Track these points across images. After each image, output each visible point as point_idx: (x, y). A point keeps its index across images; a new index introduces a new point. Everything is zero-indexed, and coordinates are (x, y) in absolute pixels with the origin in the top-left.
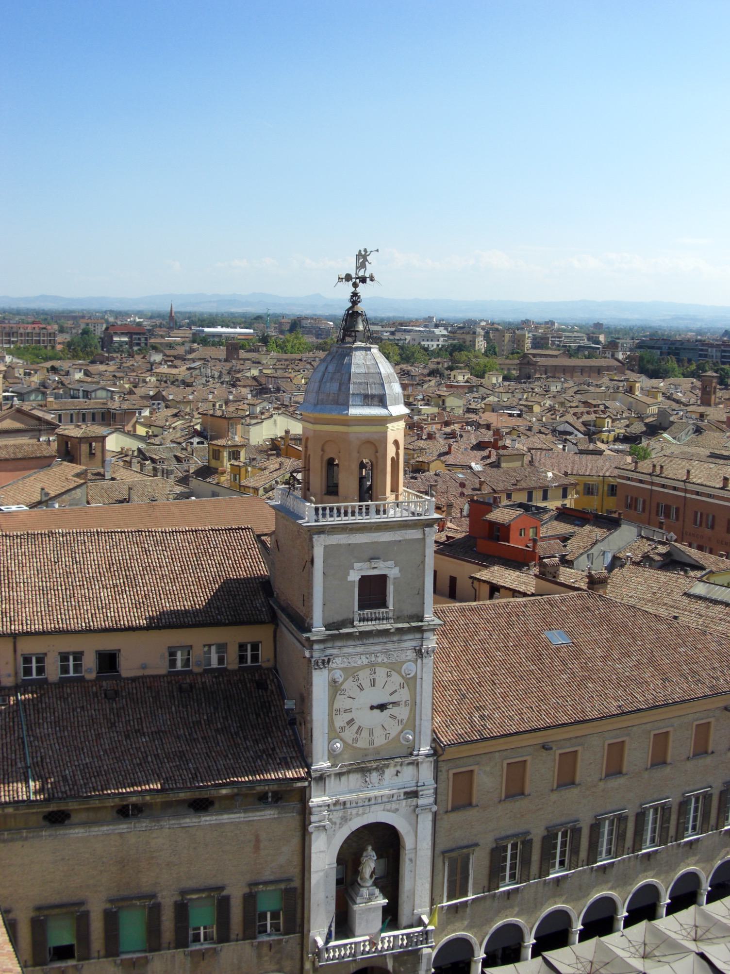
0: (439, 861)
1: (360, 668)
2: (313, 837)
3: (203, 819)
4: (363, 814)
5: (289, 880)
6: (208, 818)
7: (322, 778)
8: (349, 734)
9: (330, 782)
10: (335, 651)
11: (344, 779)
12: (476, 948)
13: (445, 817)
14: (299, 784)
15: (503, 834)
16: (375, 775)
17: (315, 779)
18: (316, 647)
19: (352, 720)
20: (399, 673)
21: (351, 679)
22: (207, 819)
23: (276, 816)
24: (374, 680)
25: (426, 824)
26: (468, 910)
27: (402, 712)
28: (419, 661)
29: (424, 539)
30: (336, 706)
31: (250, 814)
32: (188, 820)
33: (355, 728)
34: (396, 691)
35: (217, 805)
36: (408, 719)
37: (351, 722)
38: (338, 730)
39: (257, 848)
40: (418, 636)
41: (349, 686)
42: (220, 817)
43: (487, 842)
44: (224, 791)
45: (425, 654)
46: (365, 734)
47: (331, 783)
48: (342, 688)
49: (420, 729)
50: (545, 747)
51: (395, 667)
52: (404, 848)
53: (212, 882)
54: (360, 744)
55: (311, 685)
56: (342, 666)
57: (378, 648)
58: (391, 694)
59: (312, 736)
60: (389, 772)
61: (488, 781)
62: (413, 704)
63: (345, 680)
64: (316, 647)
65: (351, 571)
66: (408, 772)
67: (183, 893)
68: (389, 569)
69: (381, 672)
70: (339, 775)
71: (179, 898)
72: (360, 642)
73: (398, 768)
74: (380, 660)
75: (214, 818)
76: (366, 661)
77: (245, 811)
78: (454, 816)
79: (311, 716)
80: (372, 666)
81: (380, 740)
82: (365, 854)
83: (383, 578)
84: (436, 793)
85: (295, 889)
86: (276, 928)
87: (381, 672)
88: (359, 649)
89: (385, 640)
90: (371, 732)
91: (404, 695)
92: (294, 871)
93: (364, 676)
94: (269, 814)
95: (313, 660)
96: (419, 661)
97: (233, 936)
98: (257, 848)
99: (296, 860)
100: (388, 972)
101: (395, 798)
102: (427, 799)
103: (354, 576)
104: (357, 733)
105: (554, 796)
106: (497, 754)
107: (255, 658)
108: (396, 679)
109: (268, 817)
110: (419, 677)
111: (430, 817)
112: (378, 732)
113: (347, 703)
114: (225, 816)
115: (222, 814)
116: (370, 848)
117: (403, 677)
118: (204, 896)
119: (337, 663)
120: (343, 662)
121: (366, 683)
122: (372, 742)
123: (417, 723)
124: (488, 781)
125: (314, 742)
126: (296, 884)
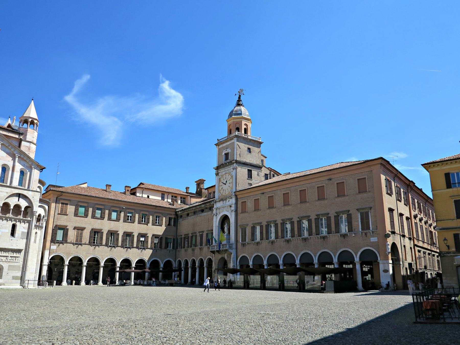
1: (223, 175)
8: (222, 192)
15: (255, 222)
22: (203, 214)
27: (231, 186)
41: (222, 179)
43: (251, 225)
50: (263, 193)
51: (229, 174)
53: (203, 230)
54: (224, 194)
60: (227, 200)
61: (250, 205)
62: (232, 183)
66: (231, 200)
68: (229, 151)
69: (227, 175)
70: (219, 201)
78: (242, 215)
80: (226, 173)
81: (227, 193)
93: (224, 176)
102: (233, 208)
103: (223, 154)
105: (268, 211)
108: (230, 177)
112: (227, 190)
121: (225, 178)
124: (250, 205)
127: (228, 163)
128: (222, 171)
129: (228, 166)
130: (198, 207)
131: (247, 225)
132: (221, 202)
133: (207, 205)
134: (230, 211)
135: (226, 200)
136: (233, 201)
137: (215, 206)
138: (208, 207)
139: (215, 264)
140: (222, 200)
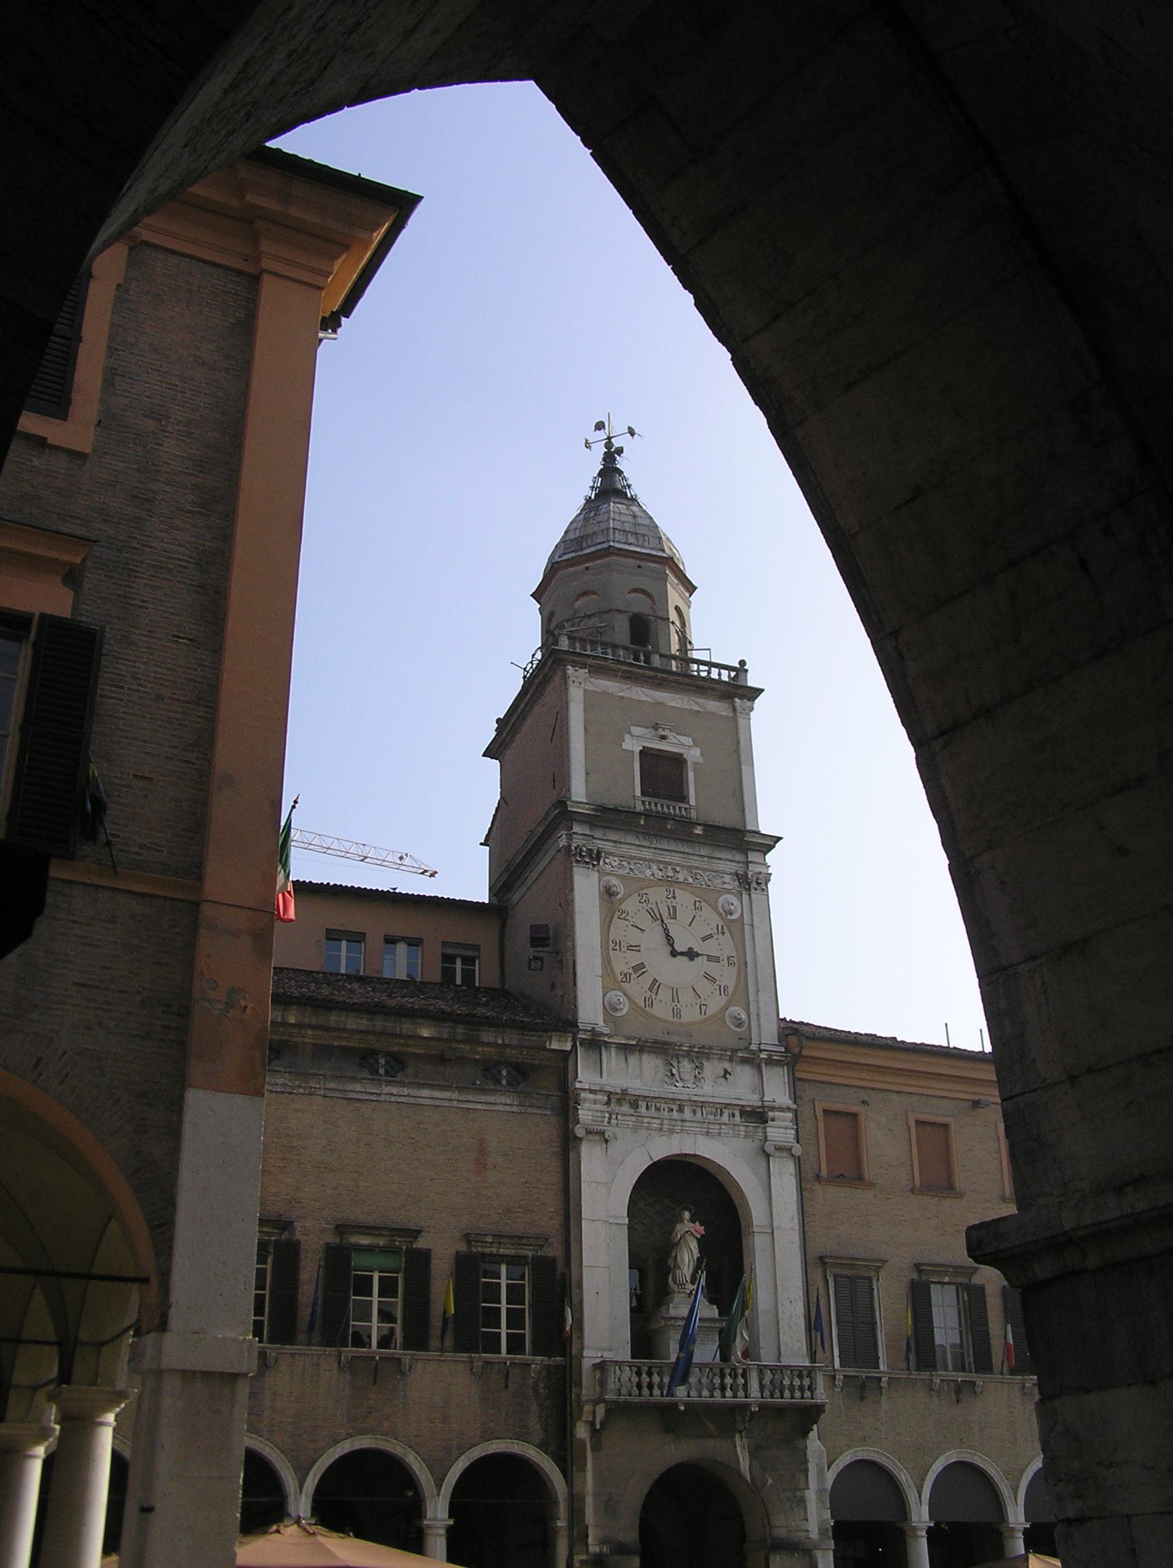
0: (817, 1274)
2: (584, 1149)
3: (386, 1090)
4: (671, 1131)
5: (543, 1240)
6: (394, 1090)
7: (595, 1043)
9: (609, 1061)
10: (607, 846)
11: (633, 1060)
12: (912, 1496)
13: (817, 1187)
14: (555, 1045)
16: (686, 1066)
17: (583, 1042)
18: (577, 828)
19: (642, 965)
20: (716, 909)
21: (635, 897)
23: (515, 1109)
24: (674, 908)
25: (784, 1177)
26: (884, 1399)
28: (745, 897)
29: (735, 718)
30: (613, 935)
31: (470, 1097)
32: (358, 1087)
33: (647, 980)
34: (711, 936)
35: (410, 1071)
36: (736, 988)
37: (640, 968)
38: (620, 978)
39: (481, 1165)
40: (739, 857)
42: (414, 1092)
44: (425, 1033)
45: (754, 885)
46: (664, 994)
47: (611, 1059)
48: (622, 907)
49: (758, 1008)
51: (706, 896)
52: (750, 1224)
55: (572, 890)
56: (620, 872)
57: (677, 859)
58: (704, 939)
59: (575, 974)
60: (712, 1068)
63: (628, 896)
64: (577, 828)
65: (627, 736)
66: (743, 1075)
67: (341, 1229)
70: (625, 1049)
71: (333, 1239)
72: (647, 843)
73: (727, 1065)
74: (681, 877)
75: (406, 1091)
76: (659, 874)
77: (460, 1089)
79: (573, 941)
81: (690, 1015)
82: (678, 1227)
83: (677, 761)
84: (796, 1120)
85: (552, 1261)
86: (516, 1344)
87: (684, 899)
88: (647, 854)
89: (687, 850)
90: (675, 995)
91: (723, 946)
92: (548, 1222)
94: (503, 1102)
95: (574, 845)
96: (745, 897)
97: (435, 1342)
98: (481, 1165)
99: (552, 1203)
100: (741, 1476)
101: (725, 1118)
102: (780, 1131)
103: (633, 745)
104: (650, 989)
106: (894, 1096)
107: (468, 975)
108: (709, 920)
109: (502, 1108)
110: (746, 919)
111: (790, 1167)
112: (686, 997)
113: (633, 937)
114: (425, 1092)
115: (420, 1086)
116: (687, 1215)
117: (720, 915)
118: (381, 1243)
119: (610, 863)
120: (621, 866)
122: (677, 1013)
123: (751, 998)
125: (579, 983)
126: (553, 1250)
127: (708, 827)
128: (634, 852)
129: (690, 839)
130: (354, 1022)
131: (878, 1265)
132: (651, 1064)
133: (487, 1036)
134: (749, 1145)
135: (699, 1055)
136: (777, 1089)
137: (585, 1076)
138: (480, 1052)
139: (608, 1506)
140: (662, 1048)
